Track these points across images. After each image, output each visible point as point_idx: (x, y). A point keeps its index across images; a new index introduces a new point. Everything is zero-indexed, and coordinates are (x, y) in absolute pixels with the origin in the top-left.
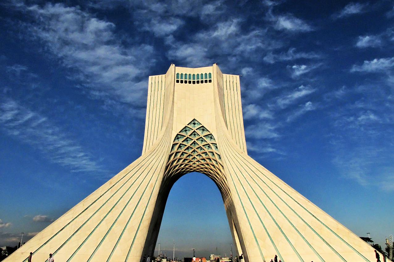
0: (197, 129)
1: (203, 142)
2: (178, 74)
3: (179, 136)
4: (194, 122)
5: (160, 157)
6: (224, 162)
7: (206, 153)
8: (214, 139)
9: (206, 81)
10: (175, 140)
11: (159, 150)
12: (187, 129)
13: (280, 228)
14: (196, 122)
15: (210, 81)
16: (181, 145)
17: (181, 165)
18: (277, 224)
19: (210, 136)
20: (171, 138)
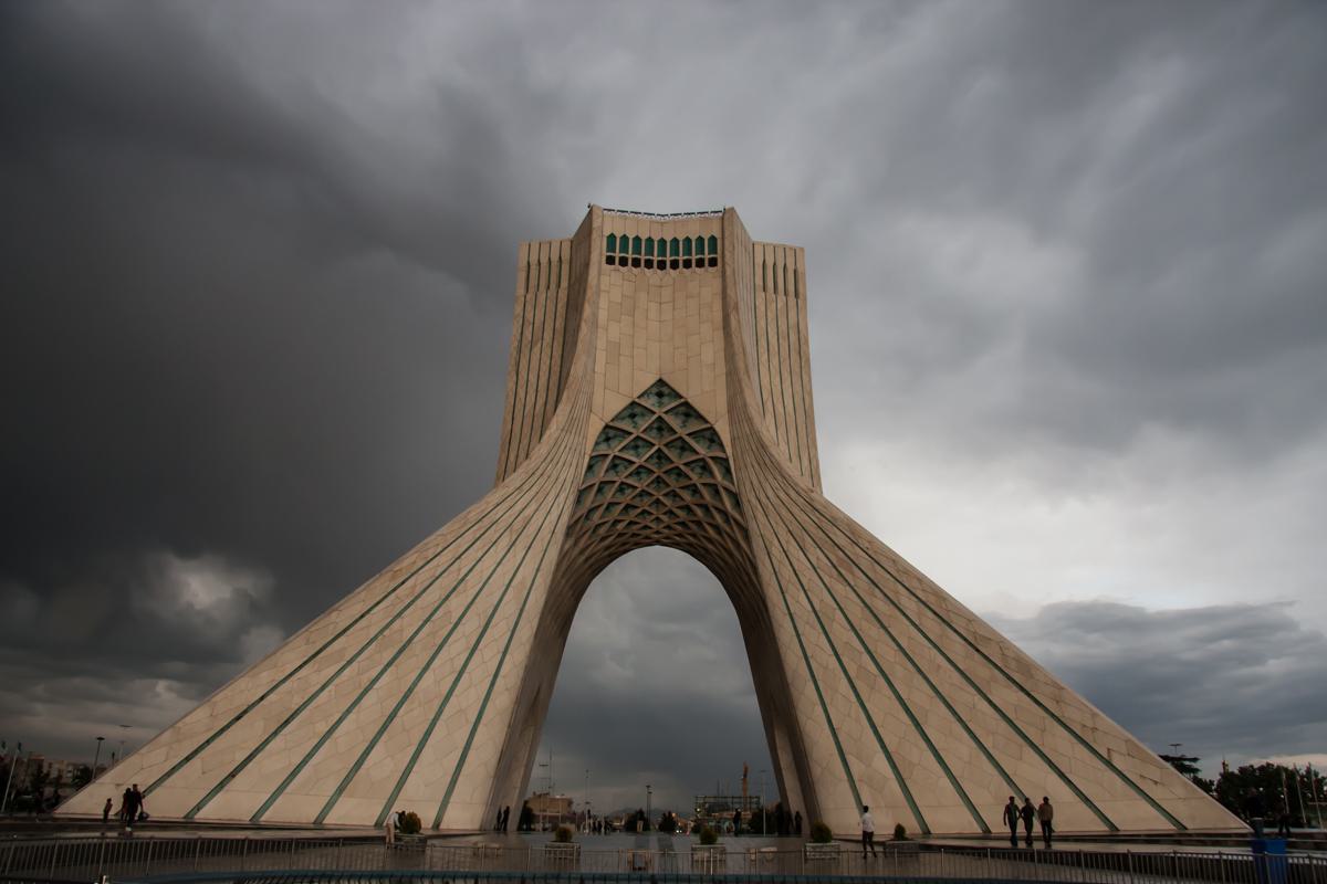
0: (666, 412)
2: (612, 237)
3: (612, 433)
4: (662, 389)
5: (551, 498)
6: (749, 513)
7: (695, 490)
8: (721, 445)
9: (700, 263)
10: (597, 444)
12: (637, 410)
13: (917, 725)
15: (713, 262)
16: (617, 462)
17: (617, 522)
19: (712, 437)
20: (585, 437)
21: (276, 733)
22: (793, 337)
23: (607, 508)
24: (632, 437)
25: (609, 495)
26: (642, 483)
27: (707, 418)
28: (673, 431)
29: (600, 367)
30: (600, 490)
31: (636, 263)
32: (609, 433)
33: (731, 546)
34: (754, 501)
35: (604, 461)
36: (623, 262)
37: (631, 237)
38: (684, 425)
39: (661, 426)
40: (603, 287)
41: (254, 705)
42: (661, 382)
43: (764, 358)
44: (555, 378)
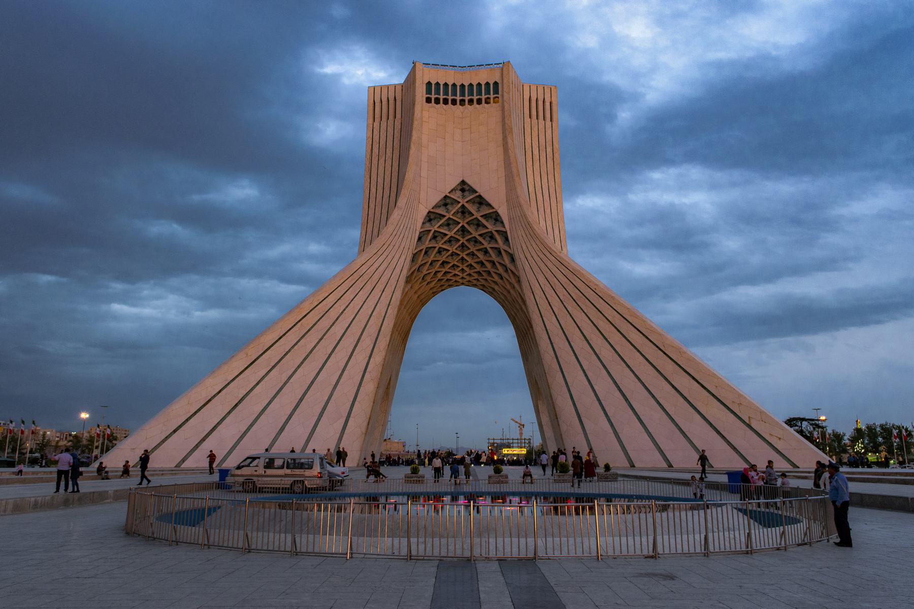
1: (480, 228)
2: (429, 84)
4: (464, 187)
7: (486, 252)
8: (502, 222)
10: (423, 223)
11: (393, 244)
12: (448, 201)
14: (466, 188)
18: (620, 390)
19: (496, 218)
21: (229, 412)
22: (549, 150)
23: (431, 264)
24: (445, 219)
25: (433, 255)
26: (453, 248)
27: (494, 205)
28: (471, 214)
29: (424, 173)
30: (426, 253)
31: (446, 102)
32: (431, 217)
33: (508, 287)
34: (522, 256)
35: (428, 234)
36: (437, 101)
37: (442, 84)
38: (478, 211)
39: (464, 211)
40: (424, 119)
41: (215, 396)
42: (463, 182)
43: (530, 163)
44: (395, 180)
